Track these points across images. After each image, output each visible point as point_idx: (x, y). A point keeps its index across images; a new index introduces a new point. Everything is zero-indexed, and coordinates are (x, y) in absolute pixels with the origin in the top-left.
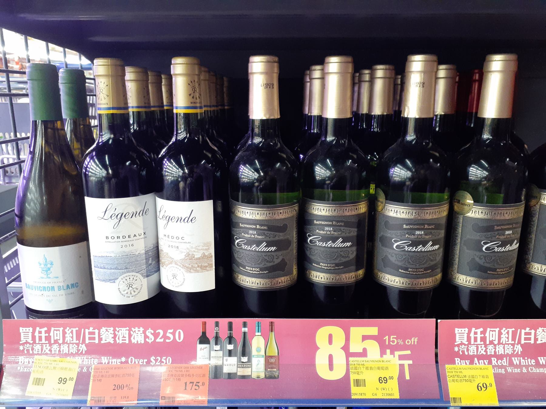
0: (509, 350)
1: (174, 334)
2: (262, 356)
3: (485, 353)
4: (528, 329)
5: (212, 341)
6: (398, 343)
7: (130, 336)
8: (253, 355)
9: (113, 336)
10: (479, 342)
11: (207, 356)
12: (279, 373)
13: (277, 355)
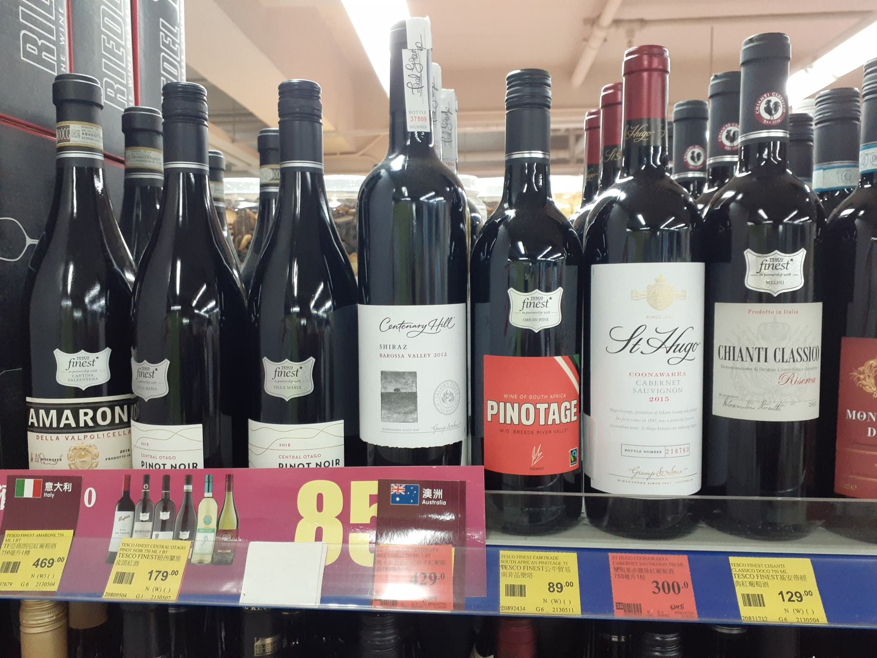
2: (212, 530)
5: (138, 506)
8: (199, 529)
11: (128, 530)
12: (234, 556)
13: (235, 528)
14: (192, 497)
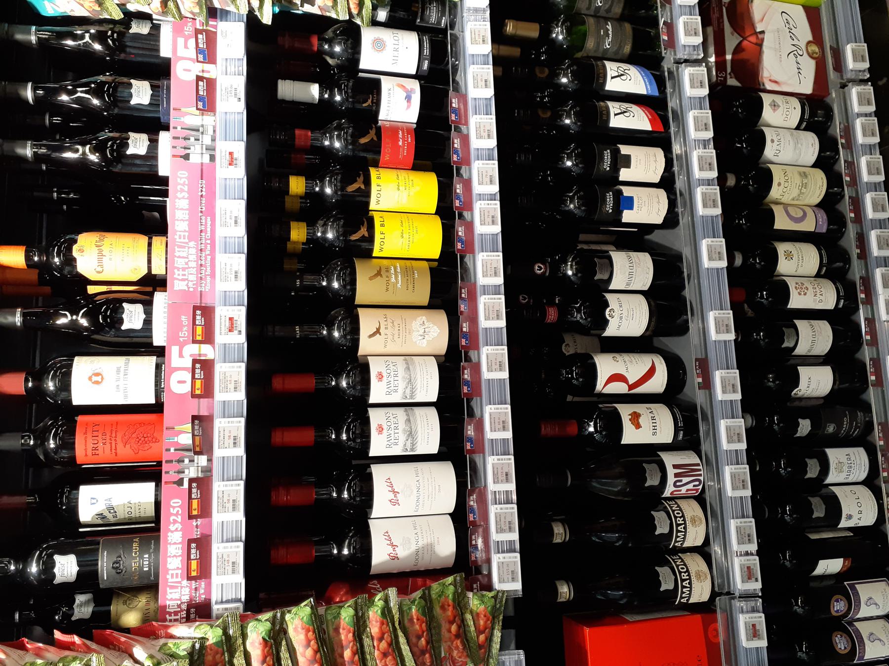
0: (193, 251)
1: (174, 508)
3: (195, 269)
4: (176, 237)
6: (186, 331)
7: (175, 543)
9: (175, 558)
10: (186, 273)
14: (177, 448)
